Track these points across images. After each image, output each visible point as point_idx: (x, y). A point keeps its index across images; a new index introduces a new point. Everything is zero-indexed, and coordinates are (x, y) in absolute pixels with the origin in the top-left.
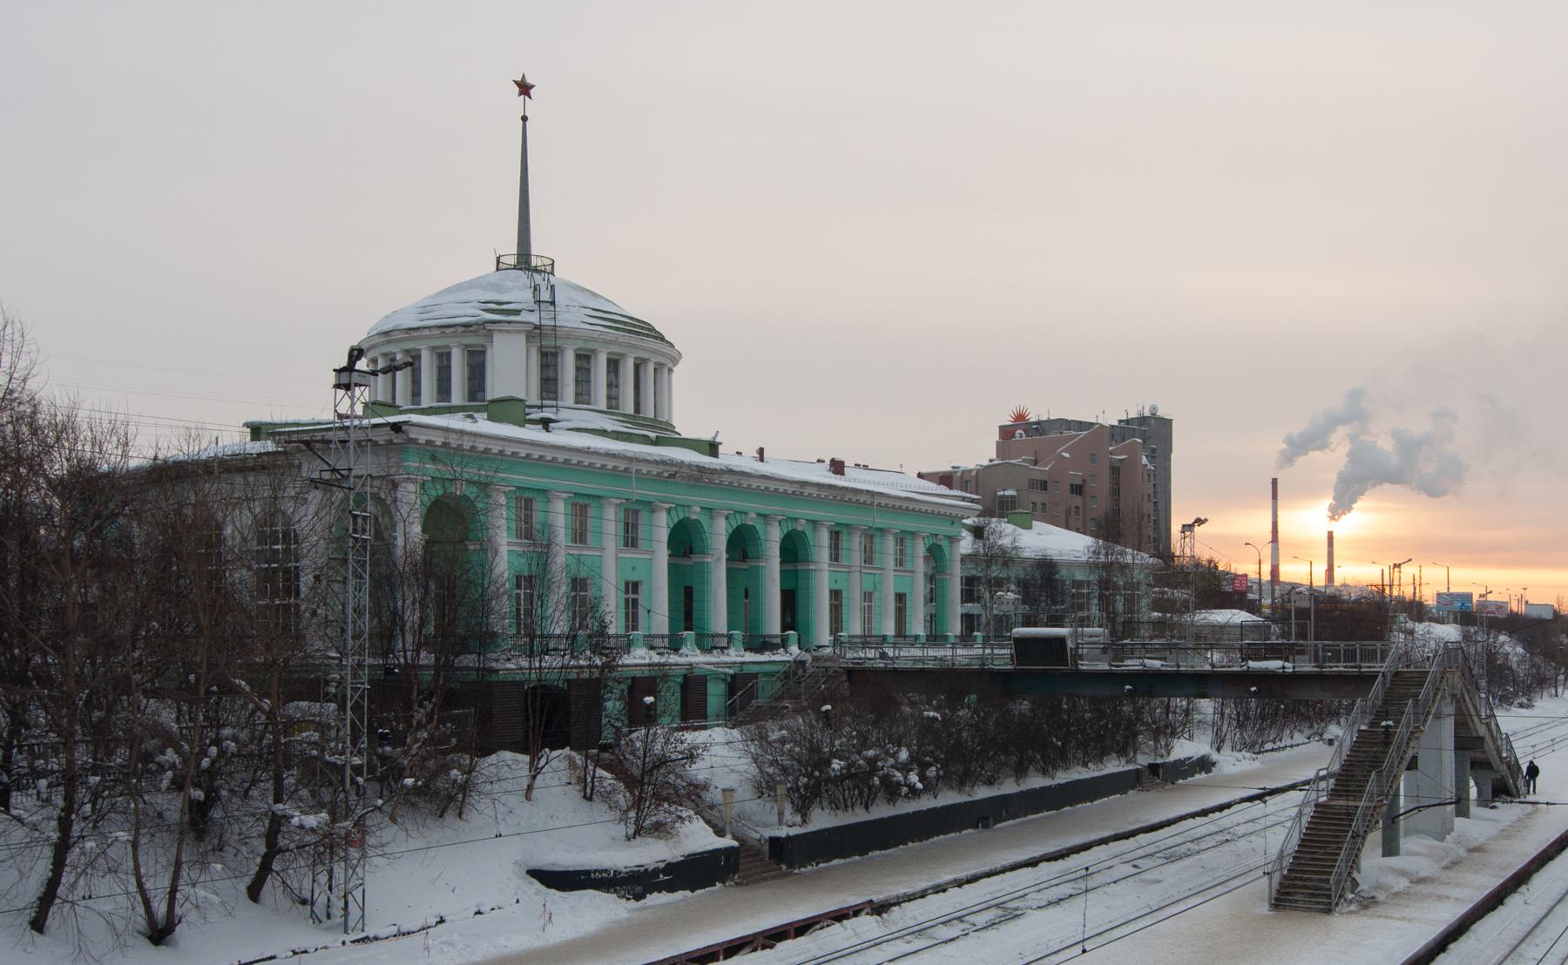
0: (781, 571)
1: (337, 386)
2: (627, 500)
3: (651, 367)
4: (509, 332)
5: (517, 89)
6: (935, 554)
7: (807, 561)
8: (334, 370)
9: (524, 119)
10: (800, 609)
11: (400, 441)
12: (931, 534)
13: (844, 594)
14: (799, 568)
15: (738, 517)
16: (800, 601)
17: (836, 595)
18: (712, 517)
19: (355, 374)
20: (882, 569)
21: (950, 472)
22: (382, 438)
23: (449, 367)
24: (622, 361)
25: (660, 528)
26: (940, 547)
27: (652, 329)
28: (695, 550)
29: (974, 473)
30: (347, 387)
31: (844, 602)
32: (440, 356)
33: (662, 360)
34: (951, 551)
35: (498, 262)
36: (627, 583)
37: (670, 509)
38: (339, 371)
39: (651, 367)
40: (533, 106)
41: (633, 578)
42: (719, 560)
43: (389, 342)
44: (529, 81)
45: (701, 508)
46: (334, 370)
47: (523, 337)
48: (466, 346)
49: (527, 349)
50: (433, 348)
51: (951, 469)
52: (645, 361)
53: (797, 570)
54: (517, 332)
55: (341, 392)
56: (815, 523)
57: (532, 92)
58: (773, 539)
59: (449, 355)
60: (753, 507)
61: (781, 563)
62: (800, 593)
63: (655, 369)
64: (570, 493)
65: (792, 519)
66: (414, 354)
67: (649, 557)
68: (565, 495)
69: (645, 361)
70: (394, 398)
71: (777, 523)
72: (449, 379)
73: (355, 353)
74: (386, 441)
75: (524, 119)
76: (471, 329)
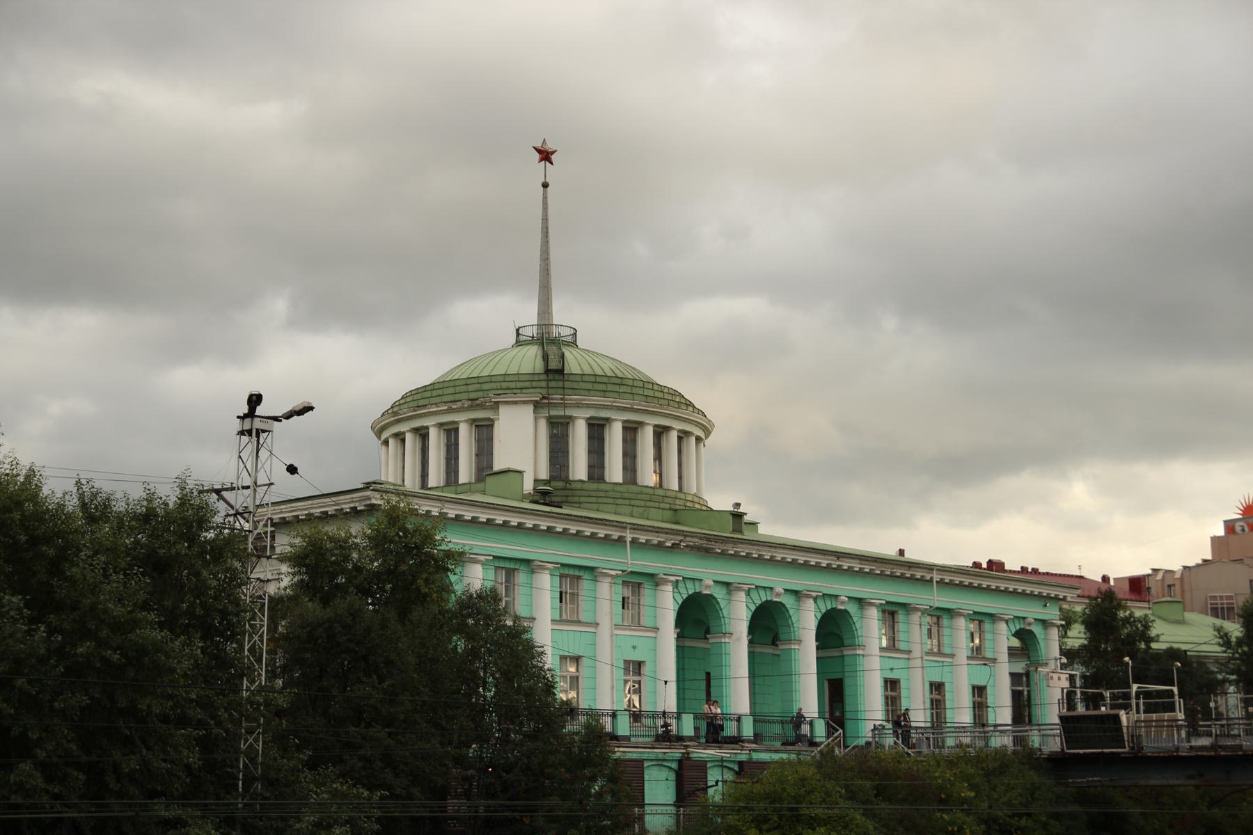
0: (817, 658)
1: (242, 433)
2: (623, 571)
3: (674, 436)
4: (516, 403)
5: (537, 156)
6: (1026, 642)
7: (854, 646)
8: (238, 417)
9: (545, 185)
10: (848, 700)
11: (362, 508)
12: (1015, 617)
13: (903, 684)
14: (845, 653)
15: (762, 592)
16: (848, 691)
17: (892, 685)
18: (729, 593)
19: (257, 420)
20: (952, 656)
21: (1149, 575)
22: (347, 506)
23: (457, 444)
24: (685, 439)
25: (667, 604)
26: (1031, 632)
27: (675, 393)
28: (712, 630)
29: (1178, 576)
30: (249, 432)
31: (904, 693)
32: (448, 432)
33: (688, 428)
34: (1046, 639)
35: (518, 334)
36: (627, 662)
37: (677, 581)
38: (243, 418)
39: (674, 436)
40: (554, 172)
41: (636, 657)
42: (739, 639)
43: (398, 421)
44: (550, 146)
45: (714, 581)
46: (238, 417)
47: (531, 408)
48: (474, 420)
49: (536, 419)
50: (441, 425)
51: (1150, 572)
52: (667, 429)
53: (843, 656)
54: (524, 402)
55: (245, 439)
56: (861, 602)
57: (553, 157)
58: (807, 621)
59: (457, 430)
60: (779, 582)
61: (818, 648)
62: (847, 682)
63: (680, 438)
64: (557, 563)
65: (830, 596)
66: (423, 432)
67: (652, 634)
68: (550, 566)
69: (667, 429)
70: (403, 481)
71: (811, 601)
72: (457, 458)
73: (254, 398)
74: (351, 508)
75: (545, 185)
76: (477, 402)
